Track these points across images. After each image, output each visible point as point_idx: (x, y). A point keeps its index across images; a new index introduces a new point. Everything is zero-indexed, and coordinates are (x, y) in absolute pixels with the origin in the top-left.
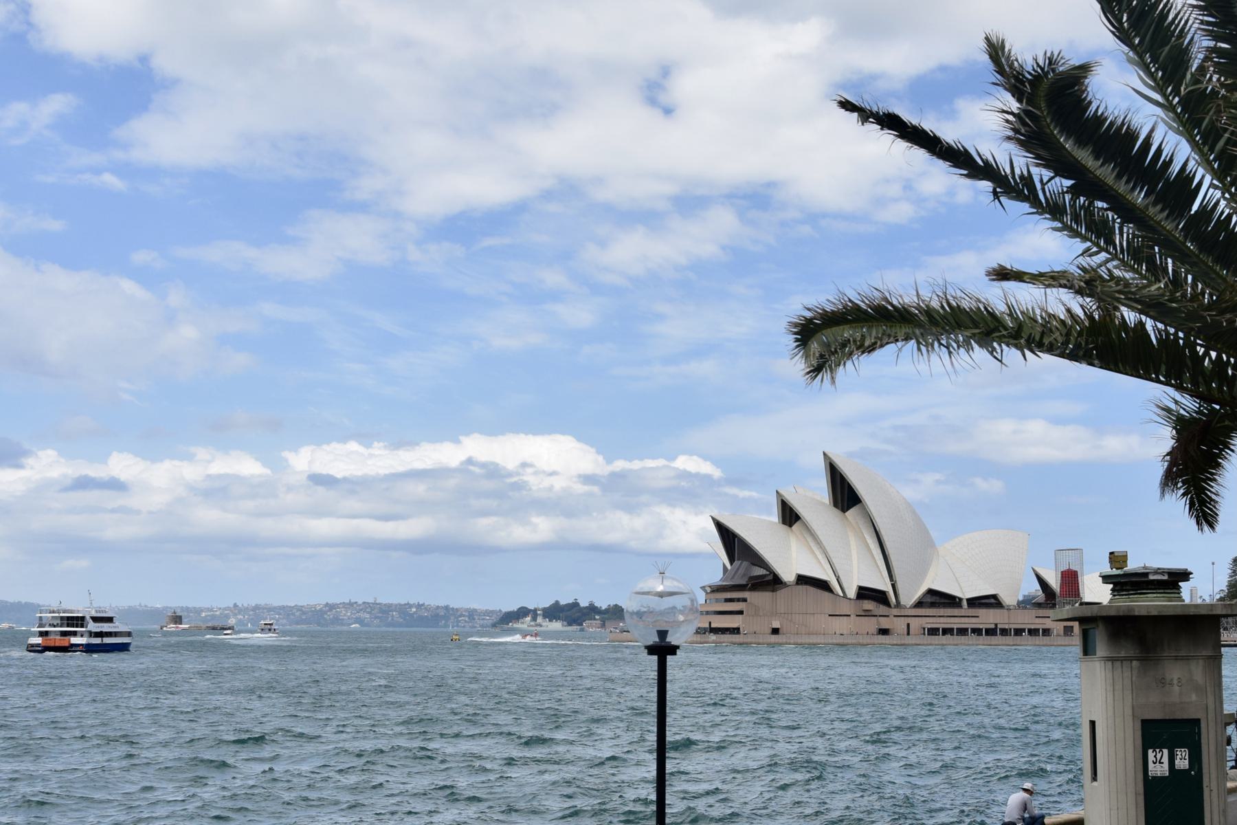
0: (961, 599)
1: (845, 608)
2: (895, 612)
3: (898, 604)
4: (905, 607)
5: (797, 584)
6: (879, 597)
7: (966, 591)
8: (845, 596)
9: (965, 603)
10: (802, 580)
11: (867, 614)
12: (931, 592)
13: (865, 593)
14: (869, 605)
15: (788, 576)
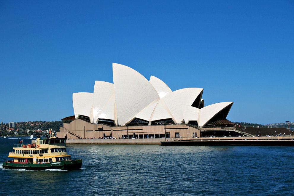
0: (148, 122)
1: (91, 127)
2: (113, 128)
3: (118, 126)
4: (121, 126)
5: (79, 119)
6: (110, 123)
7: (149, 118)
8: (93, 124)
9: (150, 123)
10: (81, 117)
11: (101, 130)
12: (136, 119)
13: (100, 122)
14: (100, 126)
15: (77, 116)
